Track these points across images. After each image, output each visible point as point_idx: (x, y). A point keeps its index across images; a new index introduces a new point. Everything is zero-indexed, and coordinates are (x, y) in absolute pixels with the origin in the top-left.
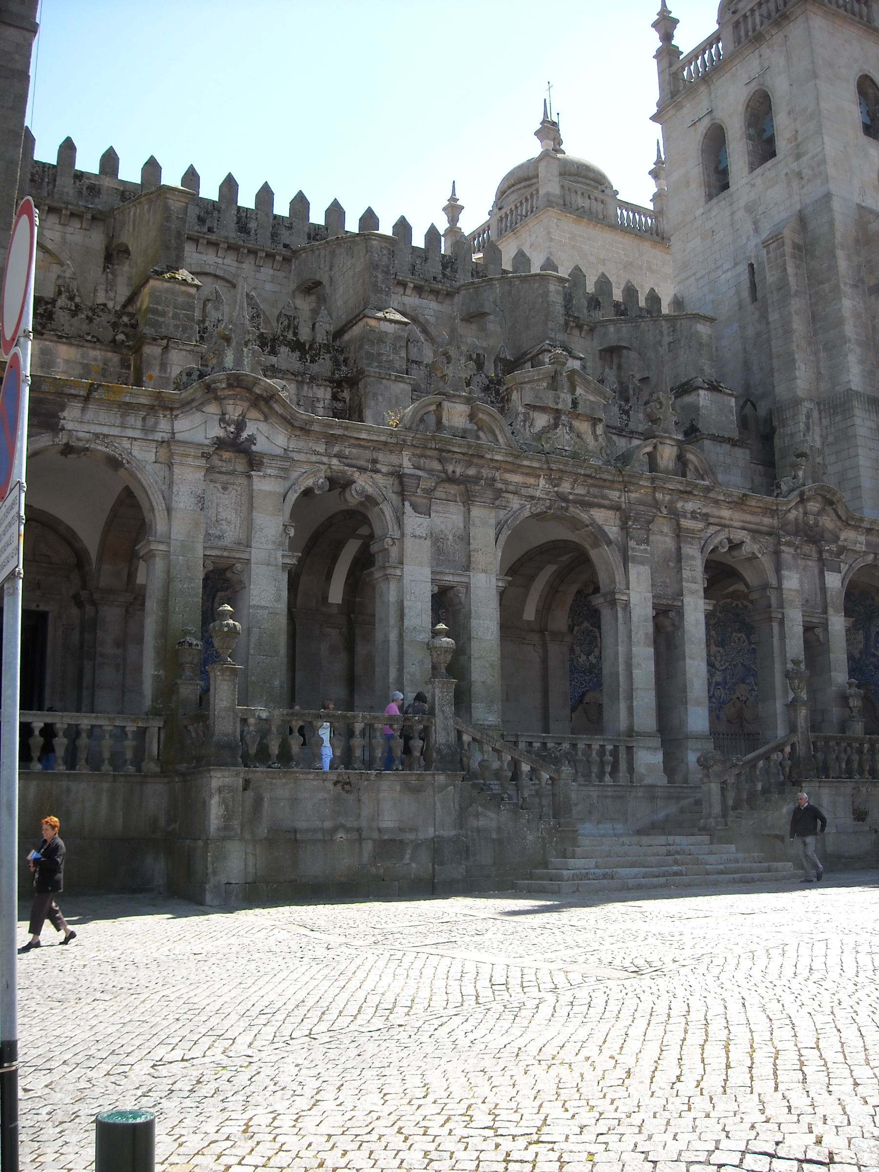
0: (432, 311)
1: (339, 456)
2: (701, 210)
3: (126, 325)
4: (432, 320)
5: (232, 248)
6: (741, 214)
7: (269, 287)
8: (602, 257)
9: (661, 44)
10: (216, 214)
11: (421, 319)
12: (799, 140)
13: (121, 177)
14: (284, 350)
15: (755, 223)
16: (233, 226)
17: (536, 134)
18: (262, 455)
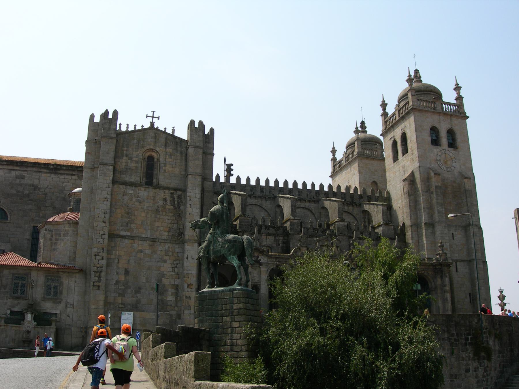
0: (313, 207)
1: (278, 261)
2: (392, 165)
3: (234, 227)
4: (313, 209)
5: (260, 197)
6: (401, 168)
7: (269, 206)
8: (376, 169)
9: (382, 111)
10: (255, 188)
11: (310, 209)
12: (413, 149)
13: (231, 182)
14: (271, 229)
15: (404, 171)
16: (259, 191)
17: (354, 132)
18: (262, 263)
